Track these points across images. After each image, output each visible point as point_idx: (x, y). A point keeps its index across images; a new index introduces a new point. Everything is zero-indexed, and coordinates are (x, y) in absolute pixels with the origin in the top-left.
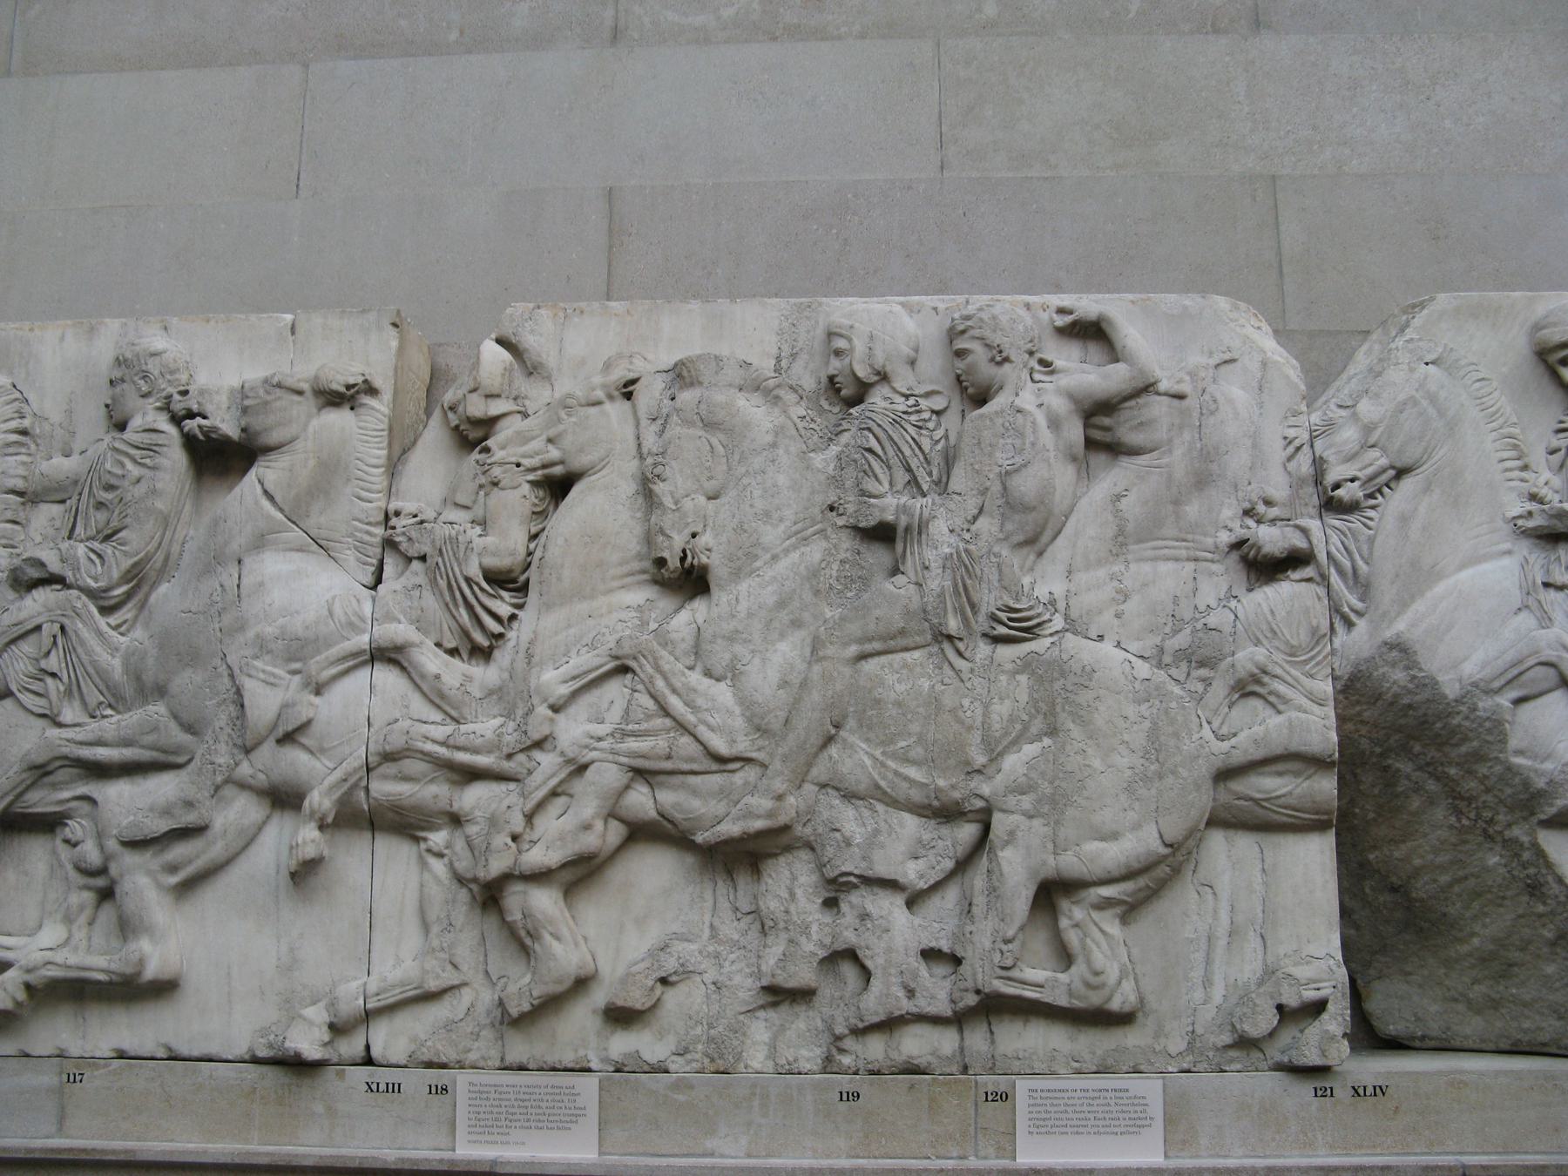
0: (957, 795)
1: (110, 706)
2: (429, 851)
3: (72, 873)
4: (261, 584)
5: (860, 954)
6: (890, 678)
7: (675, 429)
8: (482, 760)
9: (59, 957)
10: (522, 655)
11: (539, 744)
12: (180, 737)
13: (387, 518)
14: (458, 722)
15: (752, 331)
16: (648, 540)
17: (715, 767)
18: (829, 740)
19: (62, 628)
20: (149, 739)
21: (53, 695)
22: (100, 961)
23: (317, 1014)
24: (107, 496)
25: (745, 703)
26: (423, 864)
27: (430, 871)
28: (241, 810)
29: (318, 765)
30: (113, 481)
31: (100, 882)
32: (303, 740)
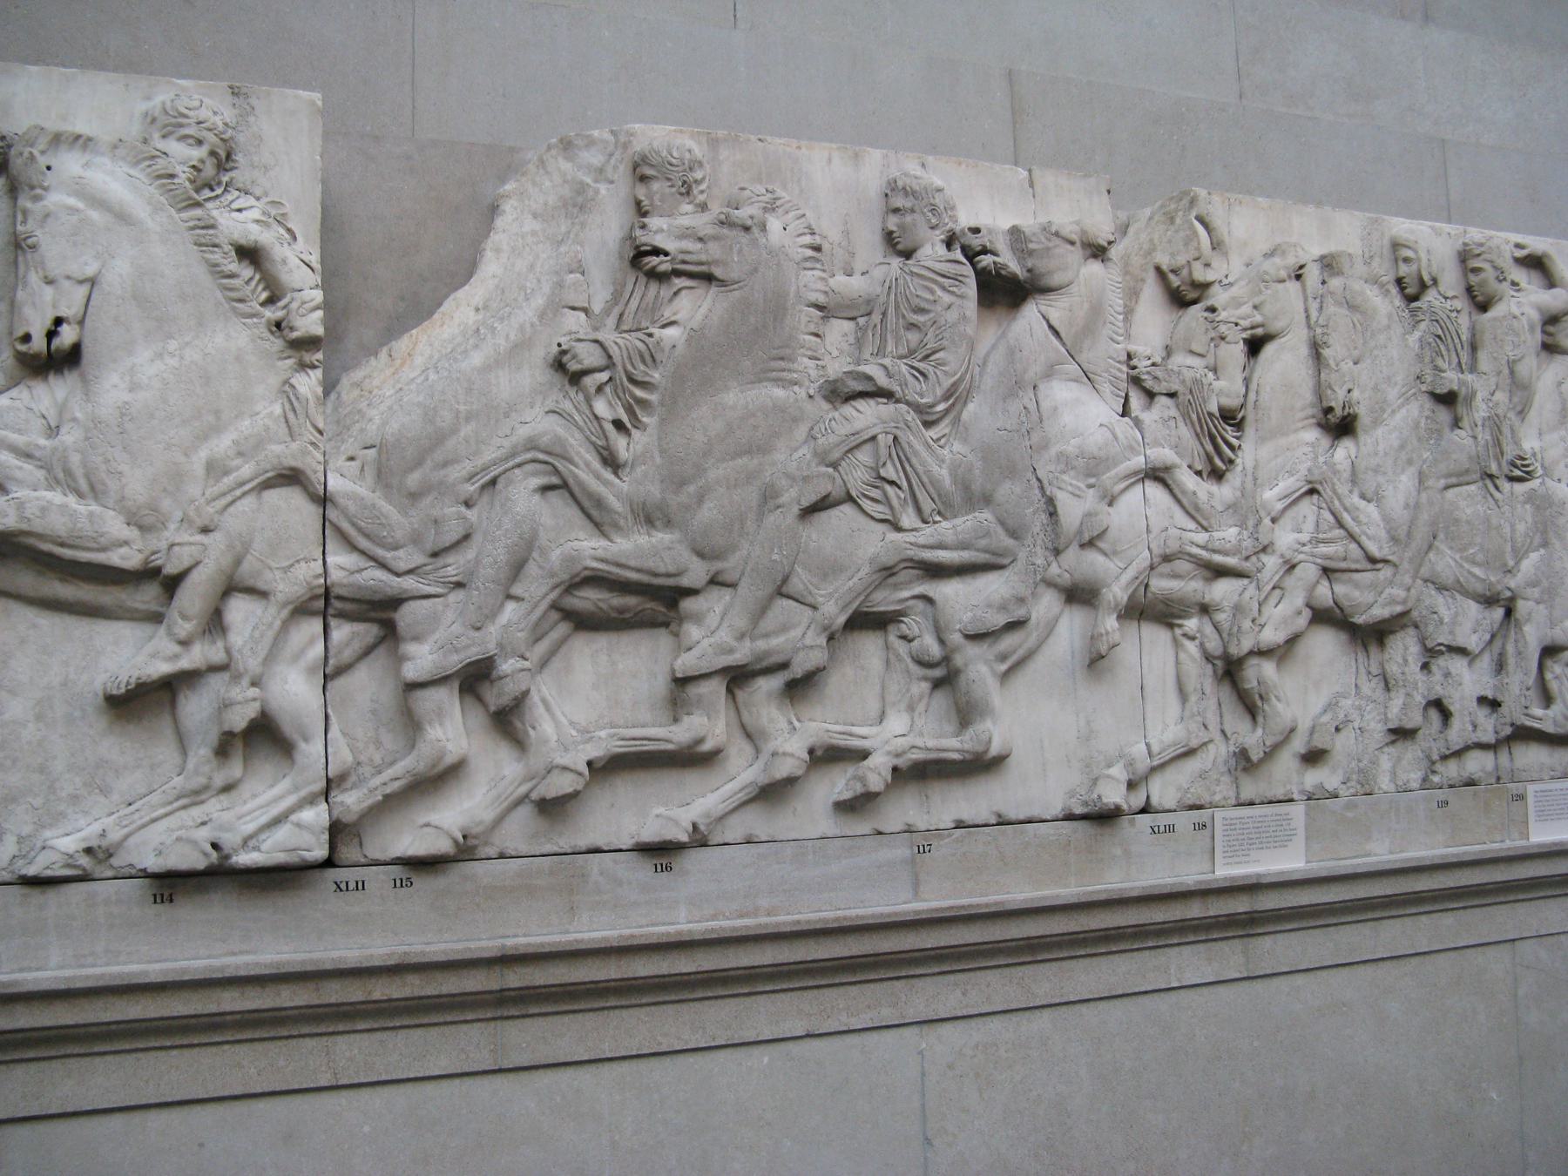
0: (1499, 587)
1: (939, 513)
2: (1184, 635)
3: (913, 667)
4: (1056, 409)
5: (1445, 701)
6: (1463, 504)
7: (1331, 309)
8: (1231, 561)
9: (919, 742)
10: (1250, 478)
11: (1264, 550)
12: (1009, 542)
13: (1130, 357)
14: (1206, 530)
15: (1345, 232)
16: (1319, 391)
17: (1369, 566)
18: (1430, 547)
19: (895, 438)
20: (983, 543)
21: (895, 502)
22: (953, 743)
23: (1119, 772)
24: (920, 319)
25: (1386, 519)
26: (1176, 643)
27: (1186, 651)
28: (1047, 604)
29: (1112, 565)
30: (923, 305)
31: (938, 673)
32: (1101, 545)
